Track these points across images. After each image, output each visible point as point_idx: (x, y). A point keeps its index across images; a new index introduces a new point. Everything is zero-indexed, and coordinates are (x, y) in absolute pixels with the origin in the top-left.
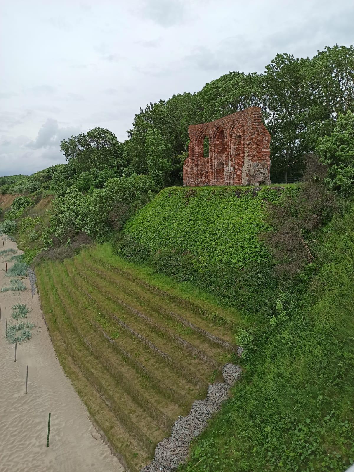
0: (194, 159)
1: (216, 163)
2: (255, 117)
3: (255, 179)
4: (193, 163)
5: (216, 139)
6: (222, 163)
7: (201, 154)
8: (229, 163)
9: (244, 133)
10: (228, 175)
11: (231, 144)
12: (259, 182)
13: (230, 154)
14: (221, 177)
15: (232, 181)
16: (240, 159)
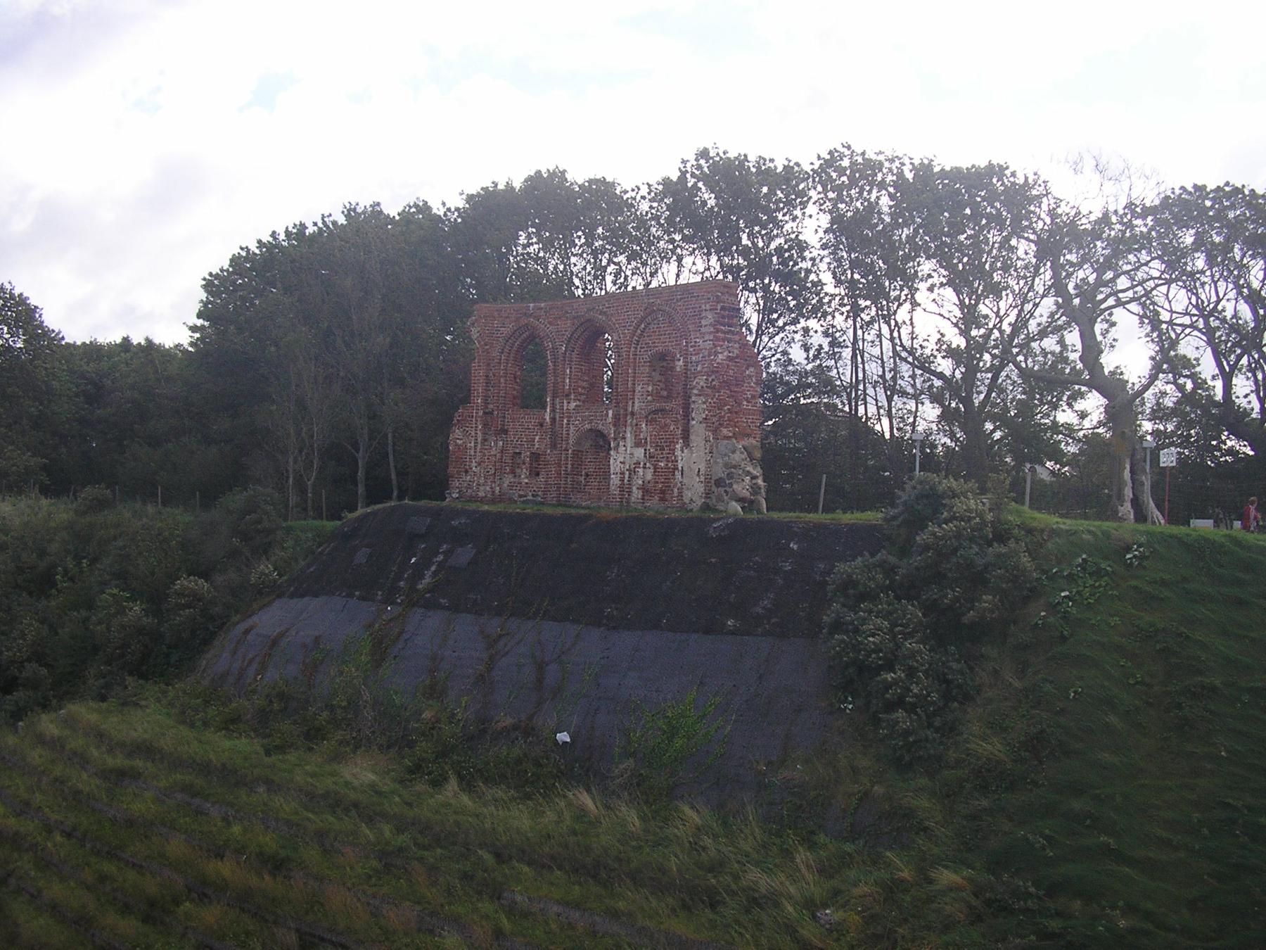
0: (491, 413)
1: (572, 432)
2: (723, 308)
3: (726, 491)
4: (485, 425)
5: (574, 355)
6: (600, 434)
7: (514, 398)
8: (629, 435)
9: (686, 350)
10: (622, 473)
11: (634, 377)
12: (740, 500)
13: (633, 406)
14: (587, 475)
15: (637, 494)
16: (666, 425)
